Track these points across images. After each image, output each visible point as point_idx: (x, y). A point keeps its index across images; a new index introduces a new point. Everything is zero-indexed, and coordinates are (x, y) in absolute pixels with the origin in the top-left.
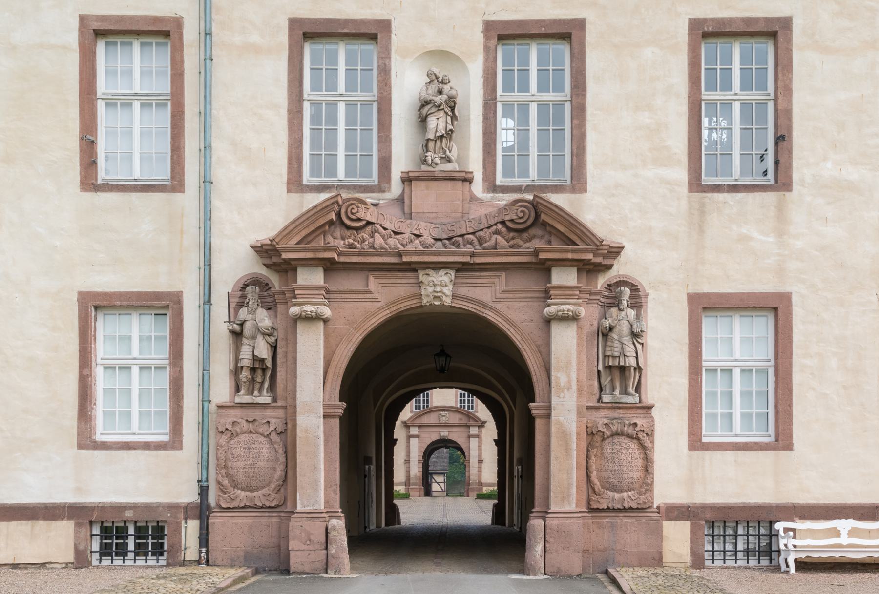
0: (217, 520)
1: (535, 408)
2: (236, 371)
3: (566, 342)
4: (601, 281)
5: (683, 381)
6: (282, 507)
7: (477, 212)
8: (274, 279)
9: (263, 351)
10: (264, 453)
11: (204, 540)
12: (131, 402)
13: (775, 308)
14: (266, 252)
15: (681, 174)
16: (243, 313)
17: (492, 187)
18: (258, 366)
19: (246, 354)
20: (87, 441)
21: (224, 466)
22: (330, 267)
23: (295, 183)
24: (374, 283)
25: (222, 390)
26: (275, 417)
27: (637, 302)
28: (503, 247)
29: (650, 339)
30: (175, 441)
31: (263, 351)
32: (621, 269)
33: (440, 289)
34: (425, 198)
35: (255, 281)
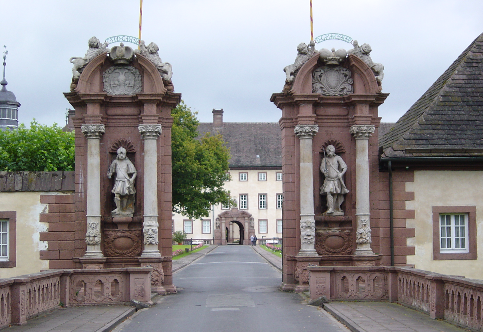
0: (215, 240)
1: (244, 230)
2: (216, 227)
3: (247, 224)
4: (250, 218)
5: (258, 227)
6: (221, 239)
7: (239, 212)
8: (220, 218)
9: (219, 225)
10: (219, 234)
11: (214, 242)
12: (207, 230)
13: (266, 220)
14: (220, 216)
15: (258, 208)
16: (217, 221)
17: (240, 209)
18: (218, 226)
19: (217, 225)
20: (202, 233)
21: (215, 235)
22: (225, 217)
23: (221, 209)
24: (229, 219)
25: (215, 228)
26: (220, 231)
27: (253, 220)
28: (241, 215)
29: (255, 224)
30: (211, 233)
31: (219, 225)
32: (252, 217)
33: (235, 219)
34: (234, 211)
35: (218, 218)
